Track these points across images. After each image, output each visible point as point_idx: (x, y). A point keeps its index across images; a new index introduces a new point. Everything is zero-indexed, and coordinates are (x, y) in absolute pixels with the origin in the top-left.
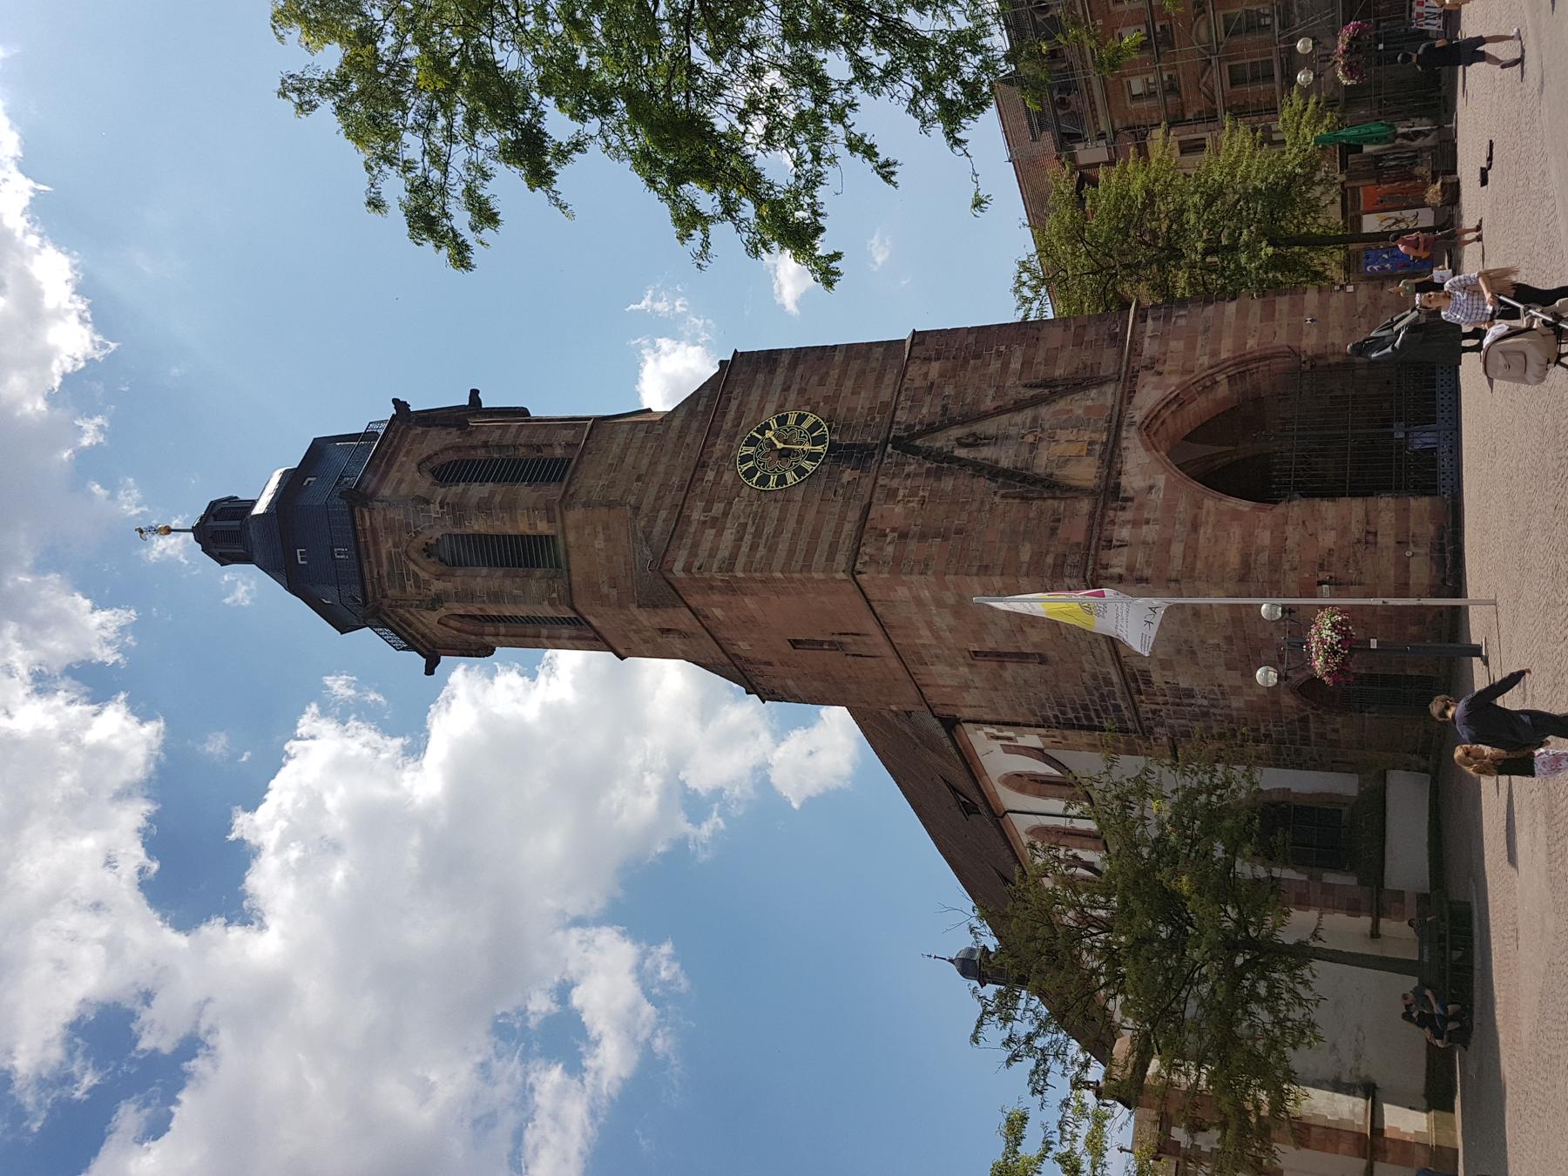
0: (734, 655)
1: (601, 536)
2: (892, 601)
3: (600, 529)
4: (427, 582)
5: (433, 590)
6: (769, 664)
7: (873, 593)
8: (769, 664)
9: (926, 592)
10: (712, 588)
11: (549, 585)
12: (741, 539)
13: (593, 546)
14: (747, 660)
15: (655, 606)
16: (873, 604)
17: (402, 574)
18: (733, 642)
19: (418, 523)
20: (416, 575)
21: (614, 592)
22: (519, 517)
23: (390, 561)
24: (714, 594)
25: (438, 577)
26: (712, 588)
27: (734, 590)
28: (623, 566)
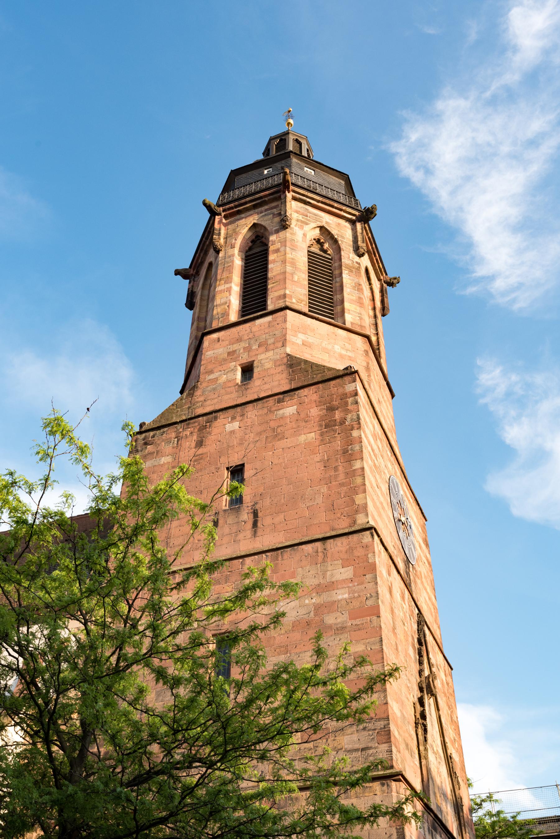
0: (216, 418)
1: (344, 352)
2: (324, 561)
3: (349, 354)
4: (301, 228)
5: (295, 228)
6: (200, 444)
7: (341, 544)
8: (200, 444)
9: (346, 596)
10: (331, 409)
11: (302, 301)
12: (372, 449)
13: (335, 344)
14: (202, 428)
15: (291, 366)
16: (318, 544)
17: (307, 216)
18: (238, 418)
19: (344, 243)
20: (307, 224)
21: (299, 342)
22: (354, 306)
23: (315, 215)
24: (321, 410)
25: (305, 235)
26: (331, 409)
27: (326, 426)
28: (321, 357)
